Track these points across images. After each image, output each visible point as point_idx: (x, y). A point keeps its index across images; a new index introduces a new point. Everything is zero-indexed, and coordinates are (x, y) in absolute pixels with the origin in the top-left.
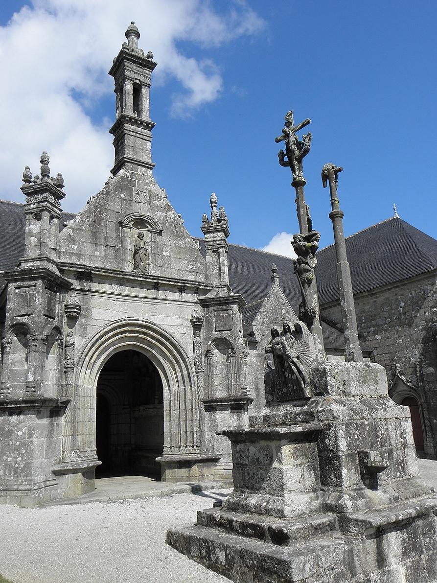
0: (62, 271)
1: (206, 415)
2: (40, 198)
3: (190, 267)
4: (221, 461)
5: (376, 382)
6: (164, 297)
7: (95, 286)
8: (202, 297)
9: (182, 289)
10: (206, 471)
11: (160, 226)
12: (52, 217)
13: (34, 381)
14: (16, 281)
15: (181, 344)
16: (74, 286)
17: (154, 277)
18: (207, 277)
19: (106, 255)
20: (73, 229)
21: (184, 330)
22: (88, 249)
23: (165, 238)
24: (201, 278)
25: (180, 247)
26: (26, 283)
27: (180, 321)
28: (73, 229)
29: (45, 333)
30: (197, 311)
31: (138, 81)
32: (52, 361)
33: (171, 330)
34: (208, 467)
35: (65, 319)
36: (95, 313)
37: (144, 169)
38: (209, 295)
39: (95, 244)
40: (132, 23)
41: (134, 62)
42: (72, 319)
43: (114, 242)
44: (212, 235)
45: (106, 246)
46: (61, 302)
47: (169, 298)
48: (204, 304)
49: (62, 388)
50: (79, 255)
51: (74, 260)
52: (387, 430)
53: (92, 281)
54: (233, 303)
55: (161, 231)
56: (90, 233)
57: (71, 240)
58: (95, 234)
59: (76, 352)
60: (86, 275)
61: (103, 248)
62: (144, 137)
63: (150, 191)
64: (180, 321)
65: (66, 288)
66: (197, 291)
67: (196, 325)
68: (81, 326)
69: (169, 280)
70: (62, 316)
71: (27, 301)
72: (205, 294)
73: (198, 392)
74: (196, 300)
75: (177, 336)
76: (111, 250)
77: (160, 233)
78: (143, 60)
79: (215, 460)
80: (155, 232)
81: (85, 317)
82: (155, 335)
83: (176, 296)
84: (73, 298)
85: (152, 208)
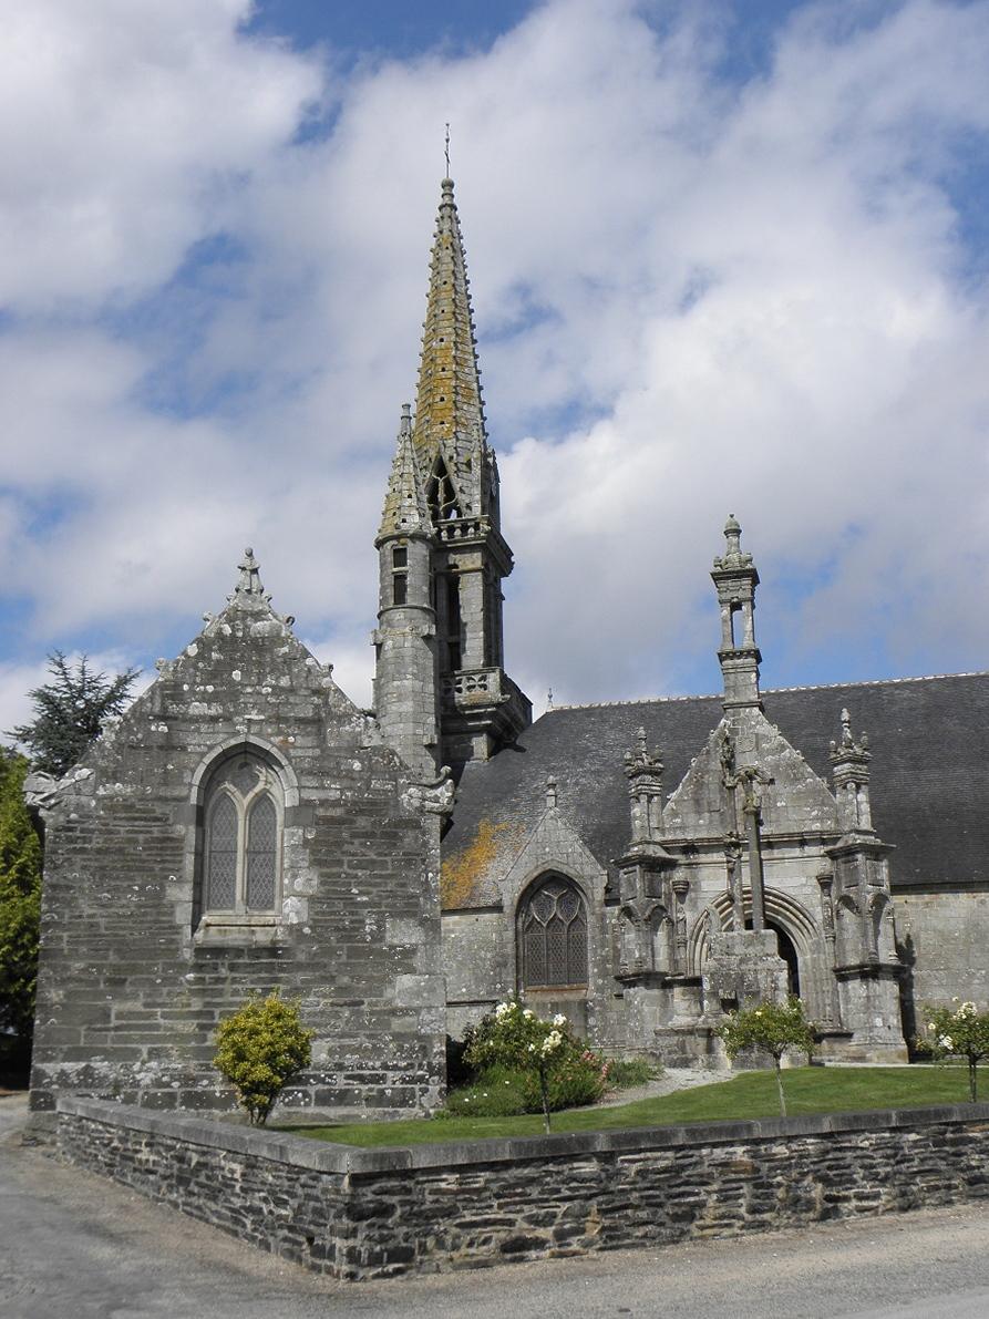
0: (667, 850)
1: (839, 984)
2: (637, 780)
3: (813, 813)
4: (855, 1036)
5: (764, 944)
6: (781, 856)
7: (703, 858)
8: (831, 847)
9: (803, 843)
10: (837, 1046)
11: (769, 775)
12: (651, 797)
13: (640, 957)
14: (623, 868)
15: (807, 906)
16: (680, 862)
17: (767, 837)
18: (837, 821)
19: (711, 822)
20: (676, 802)
21: (808, 890)
22: (691, 819)
23: (778, 785)
24: (829, 825)
25: (799, 792)
26: (630, 869)
27: (804, 880)
28: (676, 802)
29: (647, 913)
30: (825, 865)
31: (735, 600)
32: (661, 938)
33: (791, 892)
34: (841, 1043)
35: (674, 896)
36: (705, 886)
37: (747, 710)
38: (840, 844)
39: (699, 813)
40: (732, 516)
41: (728, 578)
42: (682, 895)
43: (717, 805)
44: (840, 767)
45: (710, 812)
46: (667, 880)
47: (786, 856)
48: (832, 855)
50: (683, 828)
51: (680, 836)
52: (756, 978)
53: (698, 852)
54: (858, 852)
55: (772, 781)
56: (692, 802)
57: (675, 814)
58: (697, 802)
59: (689, 928)
60: (690, 848)
61: (707, 815)
62: (747, 669)
63: (757, 735)
64: (804, 880)
65: (671, 865)
66: (823, 842)
67: (825, 883)
68: (691, 900)
69: (782, 836)
70: (670, 894)
71: (631, 886)
72: (835, 844)
73: (828, 962)
74: (822, 852)
75: (801, 899)
76: (716, 815)
77: (772, 781)
78: (738, 572)
79: (849, 1036)
80: (764, 783)
81: (695, 891)
82: (776, 900)
83: (797, 852)
84: (679, 875)
85: (761, 754)
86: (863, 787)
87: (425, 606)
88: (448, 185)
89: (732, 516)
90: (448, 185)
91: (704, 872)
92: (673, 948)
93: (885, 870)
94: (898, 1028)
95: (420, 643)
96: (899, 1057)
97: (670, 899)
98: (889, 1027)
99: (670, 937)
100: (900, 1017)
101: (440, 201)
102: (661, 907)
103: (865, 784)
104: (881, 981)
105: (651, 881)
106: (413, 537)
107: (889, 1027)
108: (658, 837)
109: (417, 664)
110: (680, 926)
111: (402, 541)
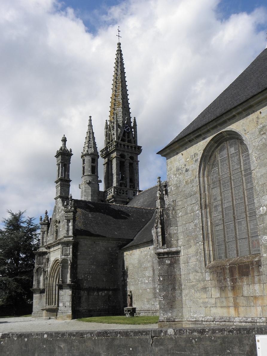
7: (52, 249)
49: (44, 284)
84: (47, 256)
86: (71, 220)
87: (89, 174)
88: (119, 44)
89: (64, 135)
90: (119, 44)
91: (52, 254)
92: (44, 280)
93: (71, 250)
94: (69, 307)
95: (87, 185)
96: (67, 317)
97: (46, 264)
98: (66, 307)
99: (44, 277)
100: (71, 302)
101: (117, 49)
102: (41, 268)
103: (71, 219)
104: (64, 290)
105: (39, 260)
106: (85, 155)
107: (66, 307)
108: (45, 244)
109: (86, 192)
110: (47, 272)
111: (83, 157)
